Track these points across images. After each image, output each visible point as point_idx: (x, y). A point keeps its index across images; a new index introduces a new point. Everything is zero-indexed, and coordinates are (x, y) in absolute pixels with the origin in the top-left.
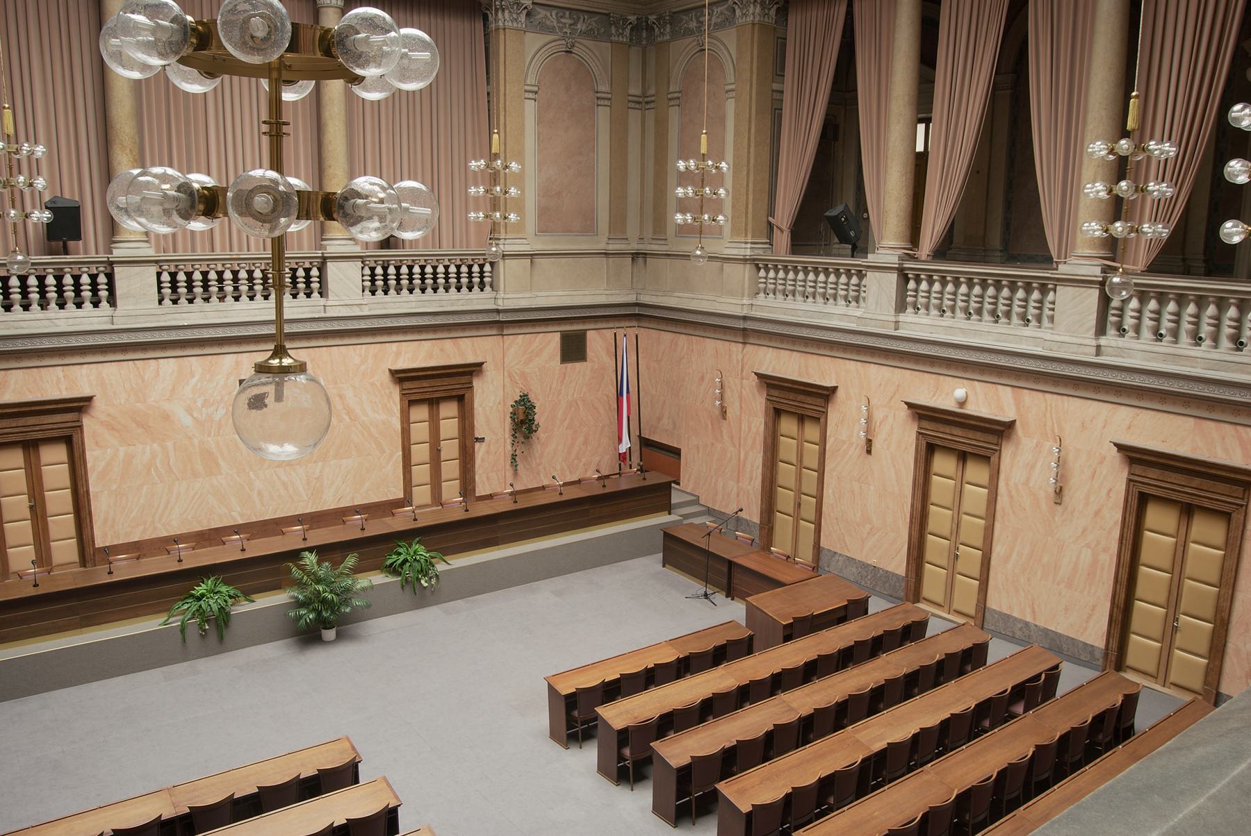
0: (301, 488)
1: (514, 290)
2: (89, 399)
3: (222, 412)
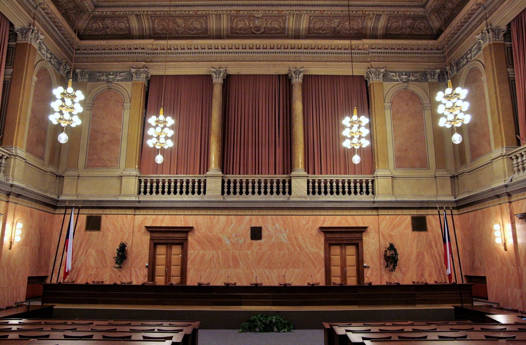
0: (275, 280)
1: (383, 193)
2: (191, 228)
3: (242, 240)
